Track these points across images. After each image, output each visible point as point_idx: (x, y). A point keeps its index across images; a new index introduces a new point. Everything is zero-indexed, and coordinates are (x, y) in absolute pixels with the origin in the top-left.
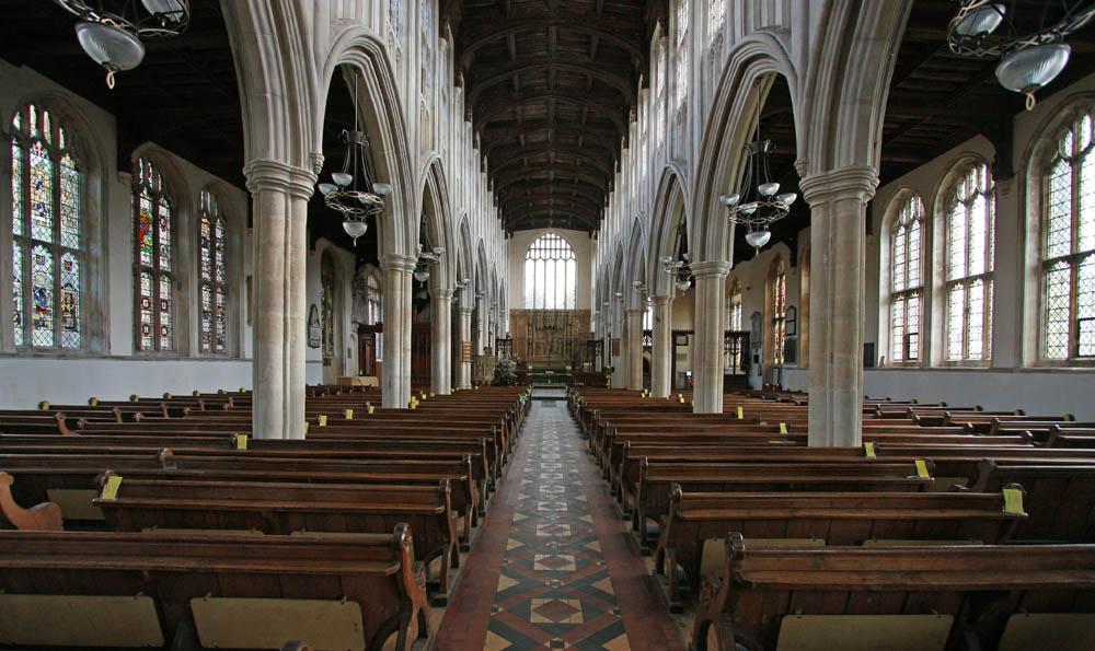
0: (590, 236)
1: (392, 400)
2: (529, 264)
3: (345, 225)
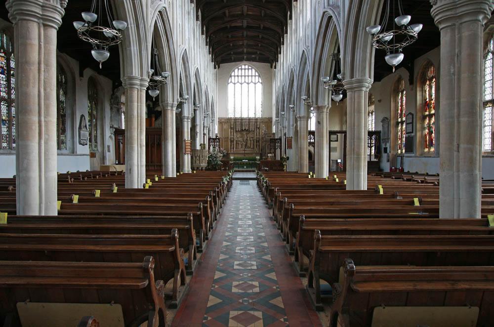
0: (272, 67)
1: (132, 182)
2: (231, 87)
3: (93, 52)
